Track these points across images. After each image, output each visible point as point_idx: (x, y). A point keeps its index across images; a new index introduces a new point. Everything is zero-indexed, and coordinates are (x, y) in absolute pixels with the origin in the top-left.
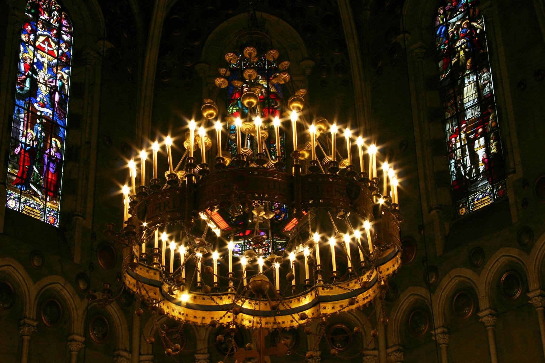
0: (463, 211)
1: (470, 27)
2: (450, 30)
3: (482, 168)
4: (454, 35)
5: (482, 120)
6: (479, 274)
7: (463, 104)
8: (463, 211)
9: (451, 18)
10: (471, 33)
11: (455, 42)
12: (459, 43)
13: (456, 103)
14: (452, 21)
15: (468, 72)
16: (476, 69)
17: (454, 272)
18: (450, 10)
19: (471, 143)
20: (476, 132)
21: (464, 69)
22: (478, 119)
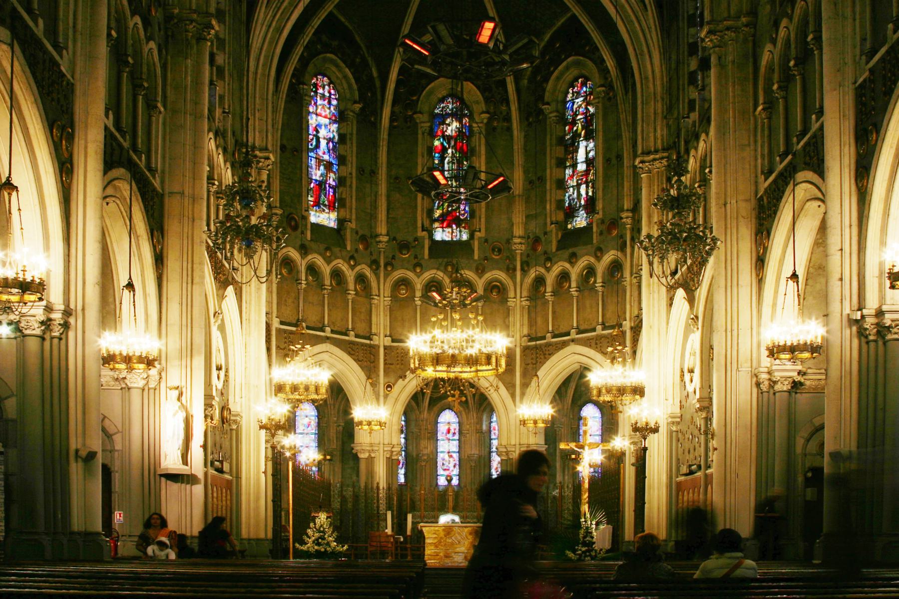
0: (569, 226)
1: (586, 109)
2: (575, 106)
3: (583, 202)
4: (576, 111)
5: (587, 173)
7: (576, 159)
8: (569, 226)
9: (576, 99)
10: (586, 113)
11: (577, 115)
12: (579, 117)
13: (573, 157)
14: (577, 101)
15: (582, 139)
16: (587, 139)
17: (560, 263)
18: (576, 92)
19: (578, 186)
20: (582, 179)
21: (580, 136)
22: (584, 171)
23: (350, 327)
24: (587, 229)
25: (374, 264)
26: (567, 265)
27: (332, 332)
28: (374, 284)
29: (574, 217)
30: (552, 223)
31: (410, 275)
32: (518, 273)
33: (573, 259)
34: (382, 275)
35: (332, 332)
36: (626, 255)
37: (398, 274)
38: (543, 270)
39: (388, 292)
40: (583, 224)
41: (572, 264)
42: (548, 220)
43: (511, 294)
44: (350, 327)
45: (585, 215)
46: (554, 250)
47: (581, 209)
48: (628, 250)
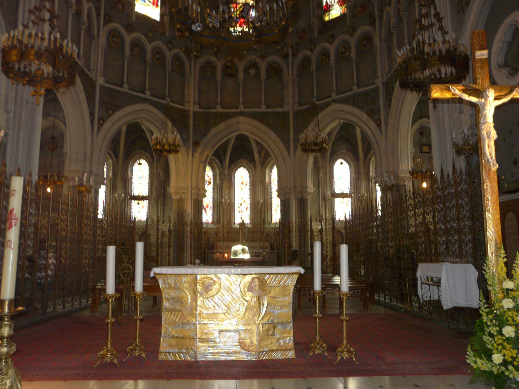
6: (331, 45)
8: (327, 19)
23: (167, 94)
24: (343, 17)
25: (188, 52)
26: (326, 45)
27: (152, 95)
28: (187, 65)
29: (330, 11)
30: (314, 17)
31: (213, 59)
32: (290, 57)
33: (331, 39)
34: (193, 62)
35: (152, 95)
36: (375, 28)
37: (203, 59)
38: (308, 52)
39: (197, 72)
40: (338, 14)
41: (331, 43)
42: (312, 15)
43: (285, 72)
44: (167, 94)
45: (339, 7)
46: (316, 36)
47: (336, 3)
48: (377, 22)
